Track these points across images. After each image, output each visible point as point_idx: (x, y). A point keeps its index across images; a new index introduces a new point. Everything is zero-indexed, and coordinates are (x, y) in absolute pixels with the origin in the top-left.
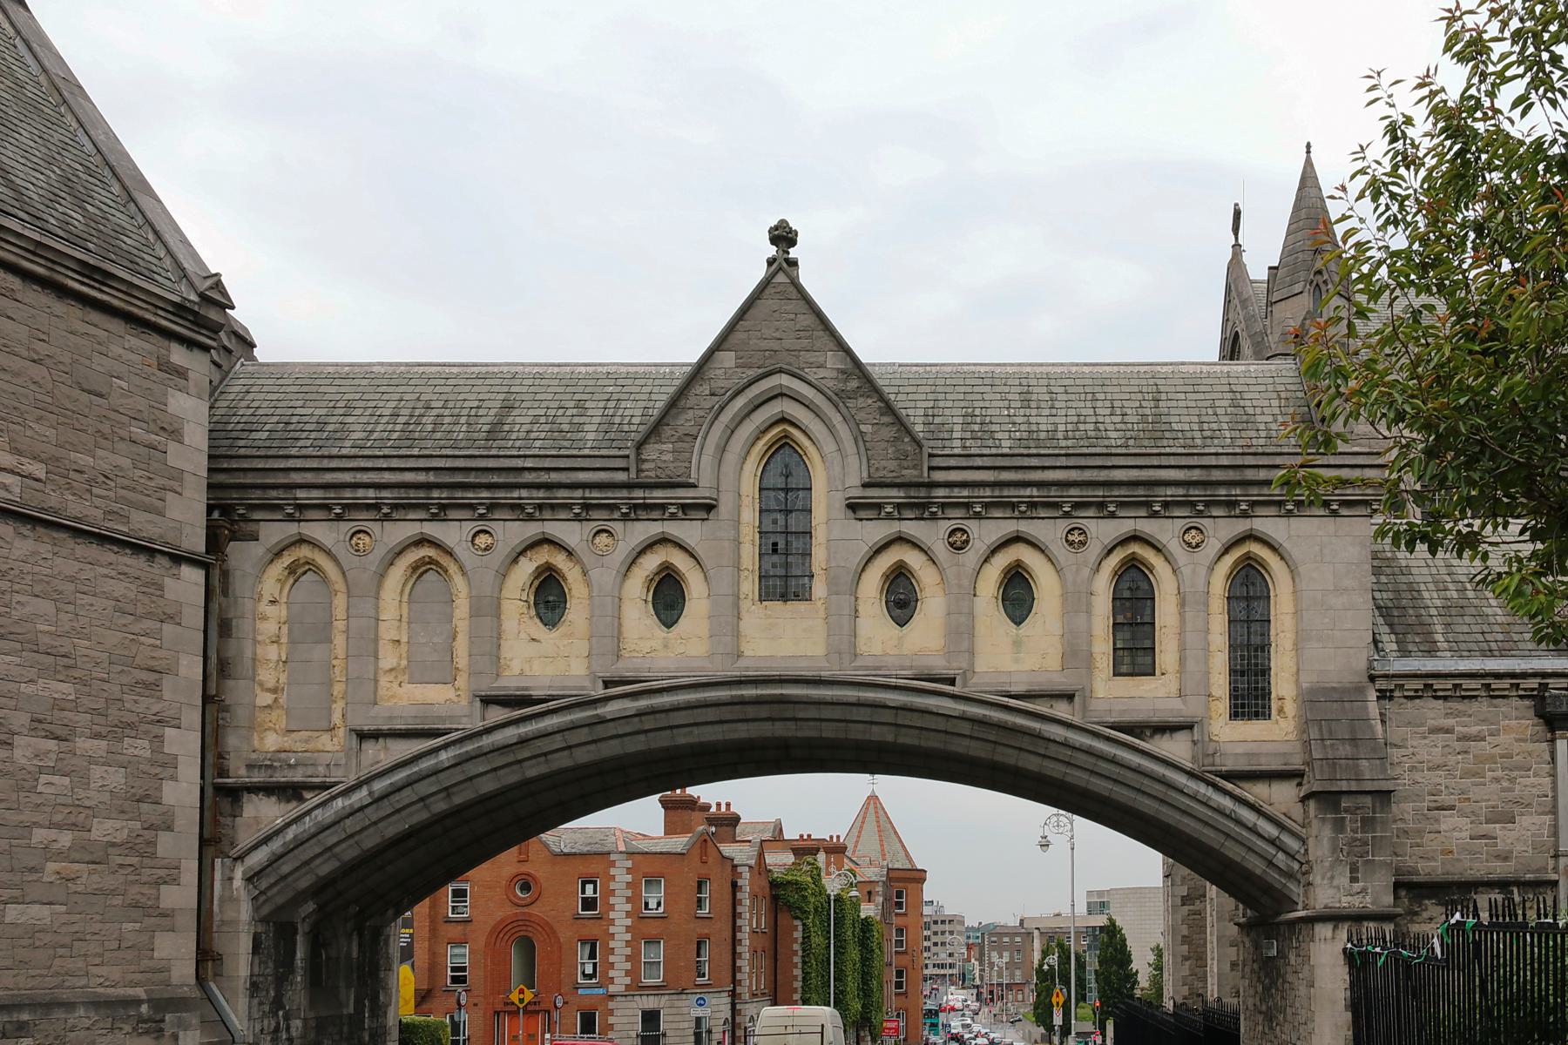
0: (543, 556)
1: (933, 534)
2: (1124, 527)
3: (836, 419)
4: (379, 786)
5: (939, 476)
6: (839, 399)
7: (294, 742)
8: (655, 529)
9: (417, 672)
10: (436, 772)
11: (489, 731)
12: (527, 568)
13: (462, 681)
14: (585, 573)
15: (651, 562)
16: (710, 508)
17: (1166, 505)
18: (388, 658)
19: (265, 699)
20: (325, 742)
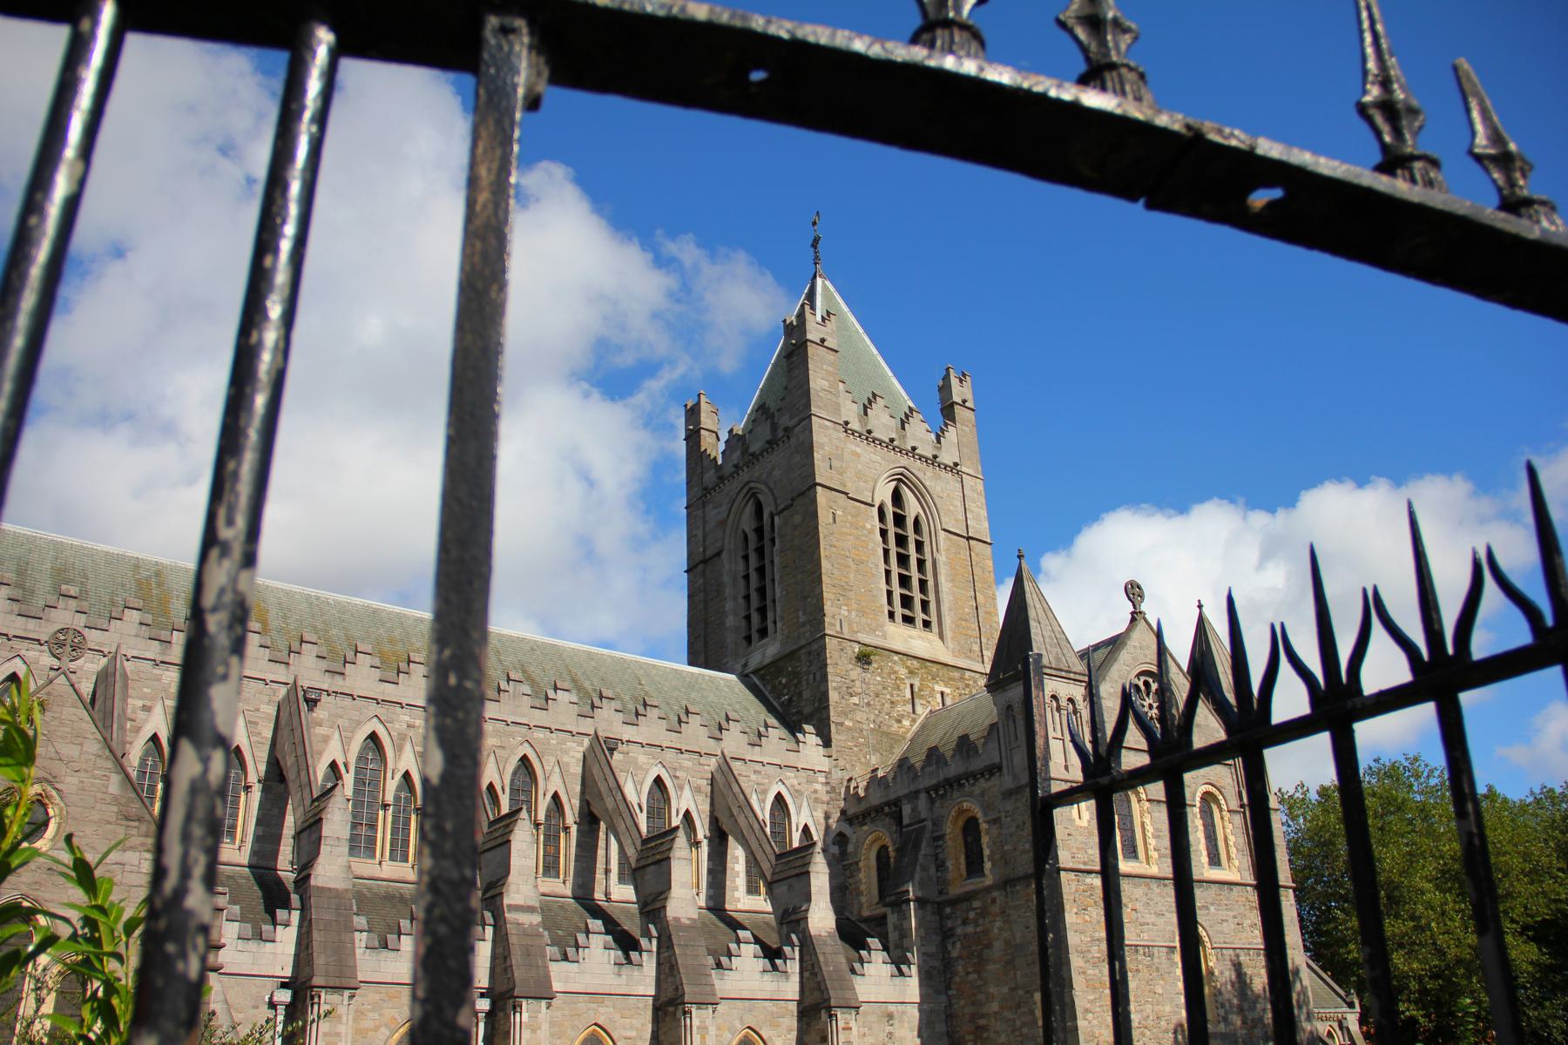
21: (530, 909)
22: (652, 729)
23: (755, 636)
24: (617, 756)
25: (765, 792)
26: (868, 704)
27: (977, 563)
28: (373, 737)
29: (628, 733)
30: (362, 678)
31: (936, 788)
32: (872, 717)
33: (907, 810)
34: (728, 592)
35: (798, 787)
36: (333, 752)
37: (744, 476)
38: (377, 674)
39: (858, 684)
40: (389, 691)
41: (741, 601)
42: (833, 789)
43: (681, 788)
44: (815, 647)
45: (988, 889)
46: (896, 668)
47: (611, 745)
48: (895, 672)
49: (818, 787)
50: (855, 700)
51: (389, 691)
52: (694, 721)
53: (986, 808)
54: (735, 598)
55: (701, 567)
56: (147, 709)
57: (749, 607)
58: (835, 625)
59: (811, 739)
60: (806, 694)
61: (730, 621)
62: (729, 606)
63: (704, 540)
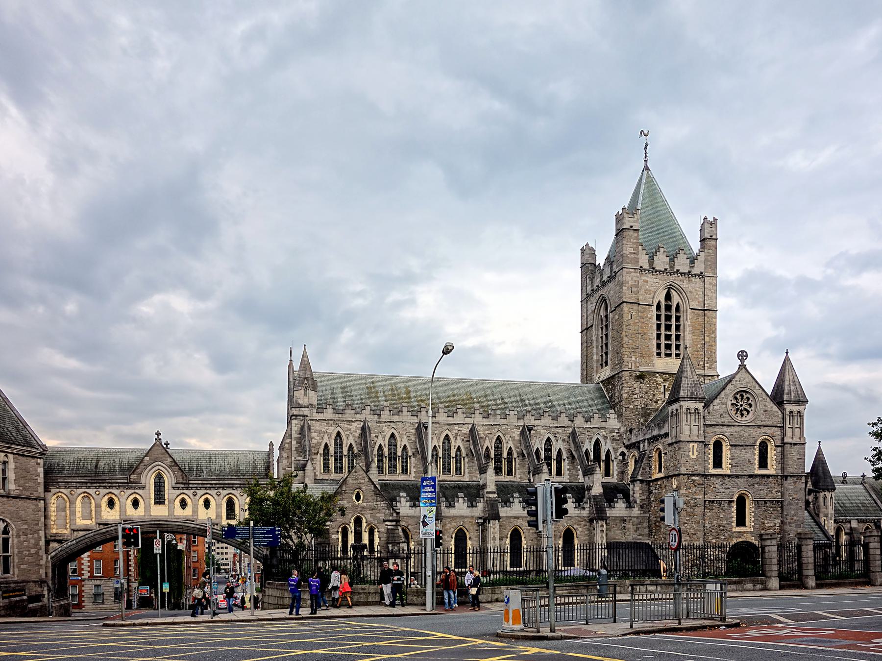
0: (110, 495)
1: (190, 492)
2: (228, 492)
3: (170, 471)
4: (77, 540)
5: (190, 482)
6: (170, 467)
7: (60, 531)
8: (133, 491)
9: (84, 518)
10: (88, 537)
11: (100, 530)
12: (106, 498)
13: (93, 520)
14: (119, 499)
15: (132, 497)
16: (144, 487)
17: (236, 488)
18: (78, 515)
19: (52, 523)
20: (65, 531)
21: (494, 493)
22: (546, 421)
23: (604, 365)
24: (532, 432)
25: (591, 438)
26: (642, 397)
27: (708, 322)
28: (447, 435)
29: (537, 423)
30: (442, 417)
31: (650, 438)
32: (643, 402)
33: (642, 446)
34: (594, 344)
35: (605, 435)
36: (435, 443)
37: (597, 295)
38: (446, 415)
39: (637, 389)
40: (451, 420)
41: (600, 348)
42: (621, 435)
43: (557, 440)
44: (620, 375)
45: (662, 478)
46: (657, 379)
47: (530, 429)
48: (657, 381)
49: (615, 434)
50: (635, 396)
51: (451, 420)
52: (563, 415)
53: (665, 449)
54: (597, 347)
55: (585, 331)
56: (377, 437)
57: (602, 352)
58: (628, 366)
59: (612, 416)
60: (616, 395)
61: (595, 357)
62: (595, 350)
63: (587, 319)
